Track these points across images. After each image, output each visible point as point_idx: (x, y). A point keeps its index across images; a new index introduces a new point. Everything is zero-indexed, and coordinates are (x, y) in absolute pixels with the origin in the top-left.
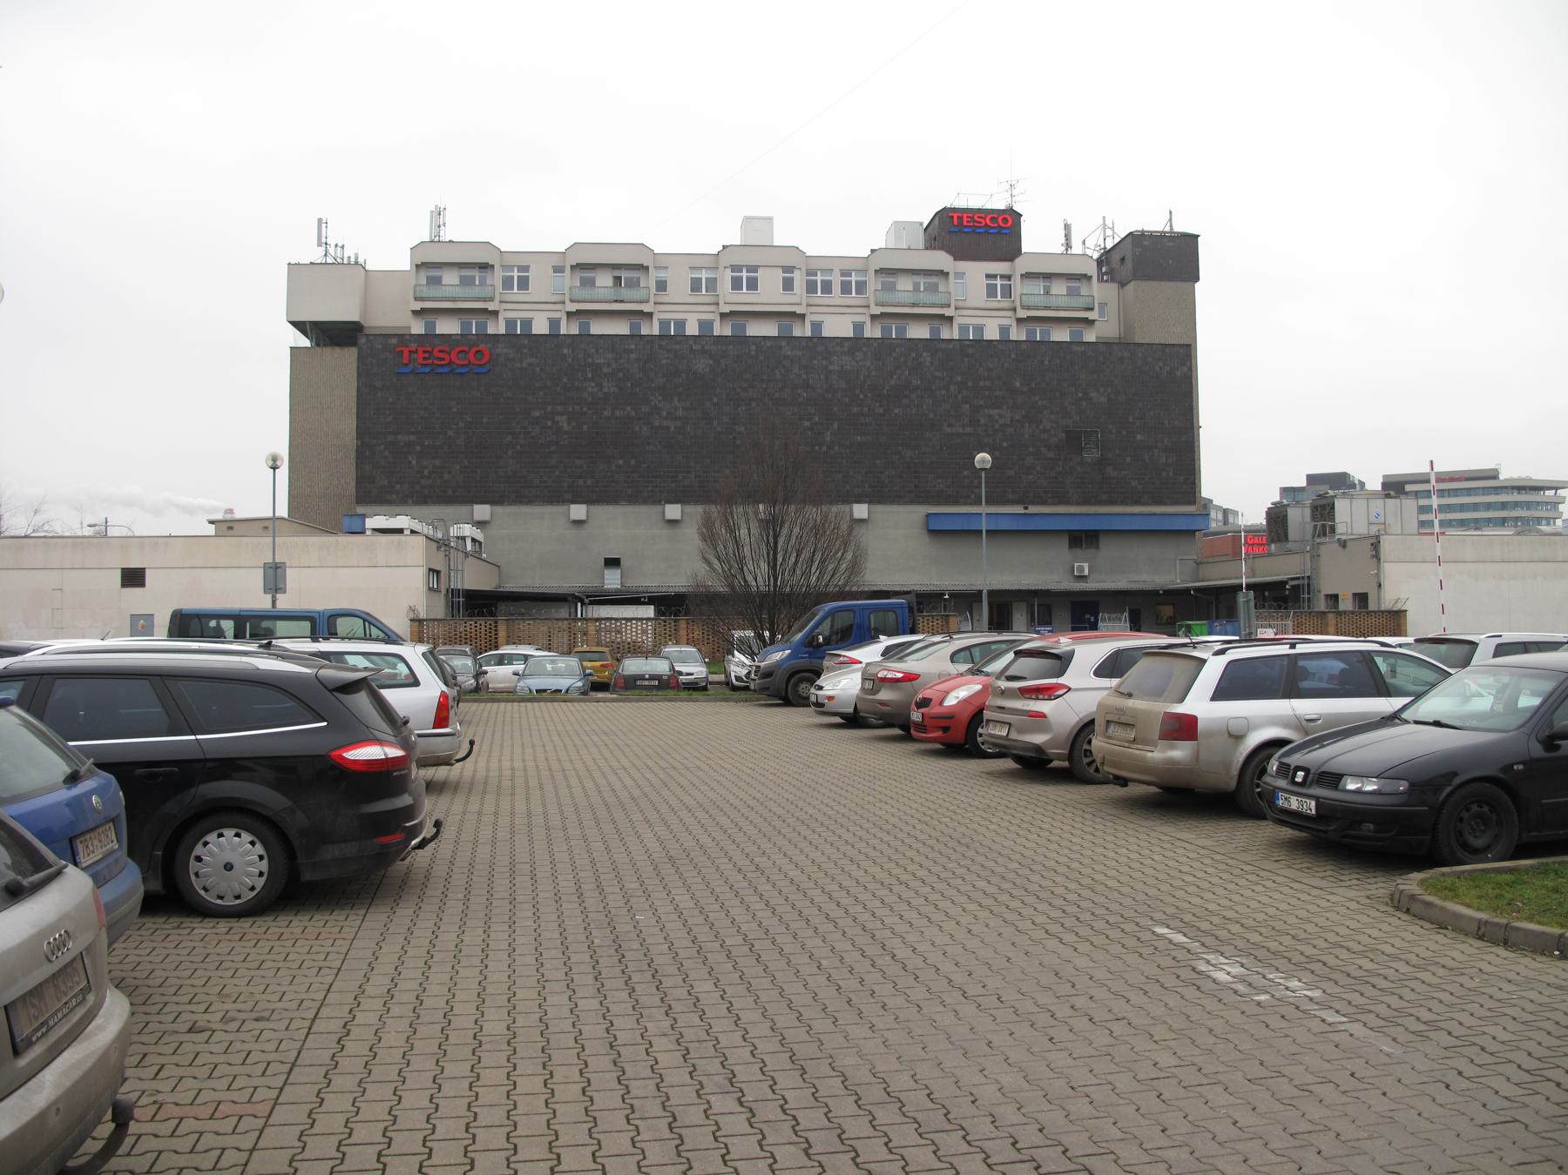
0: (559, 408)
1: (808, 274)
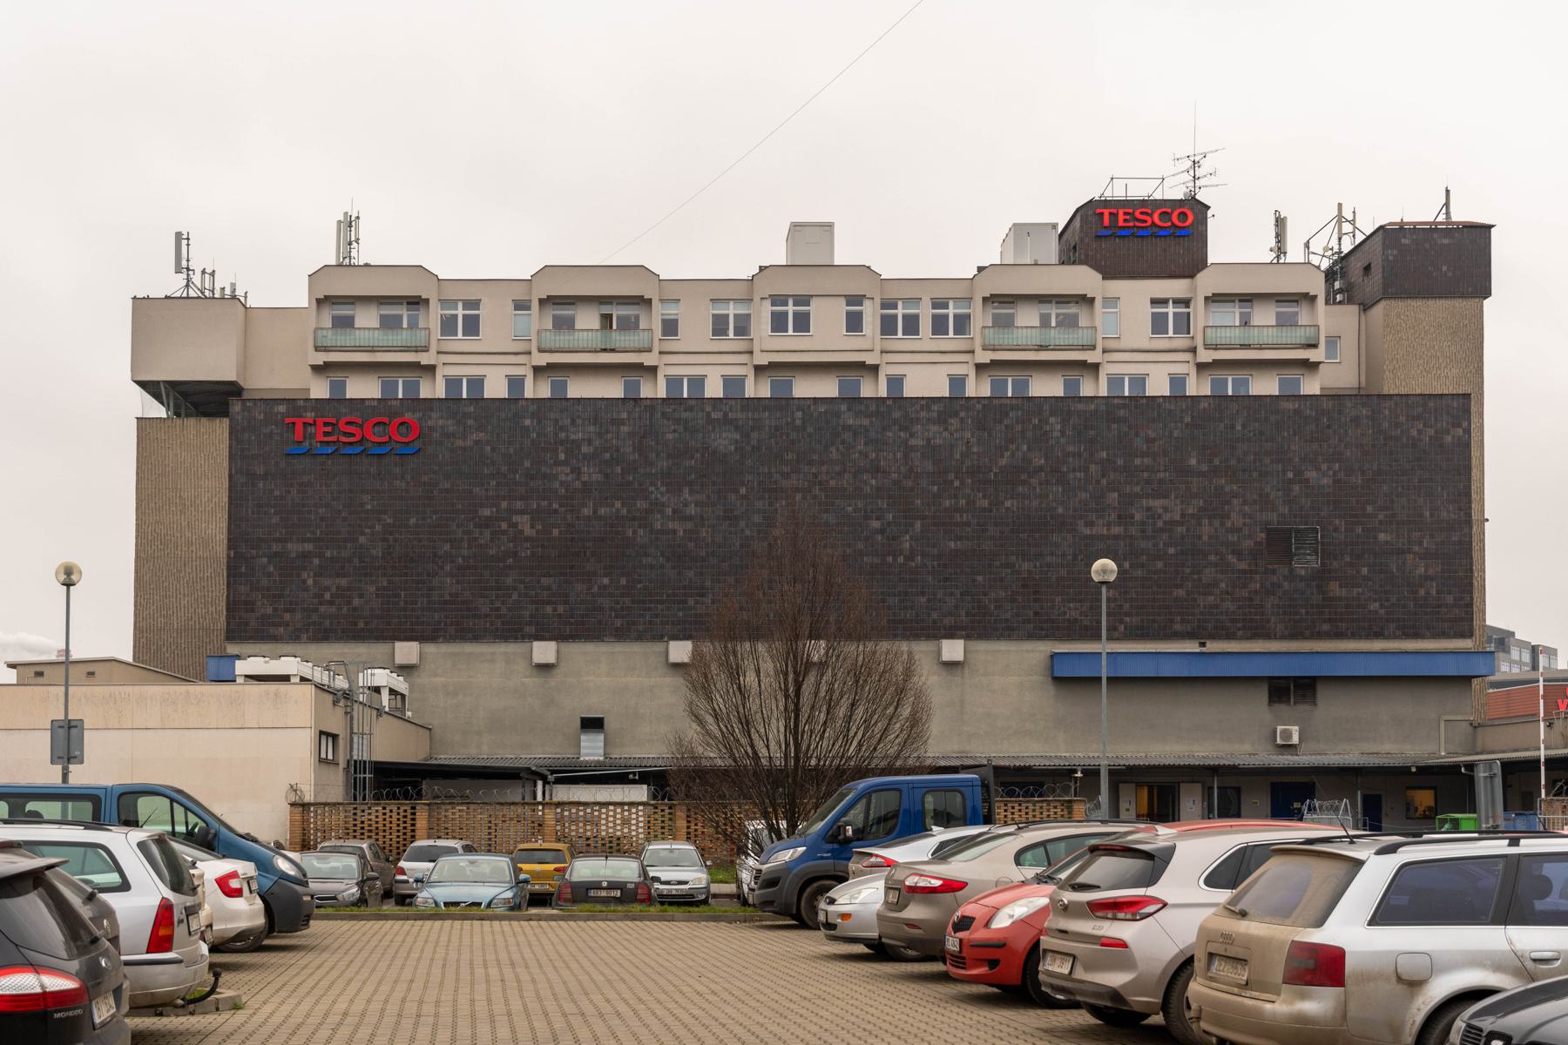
0: (519, 505)
1: (883, 306)
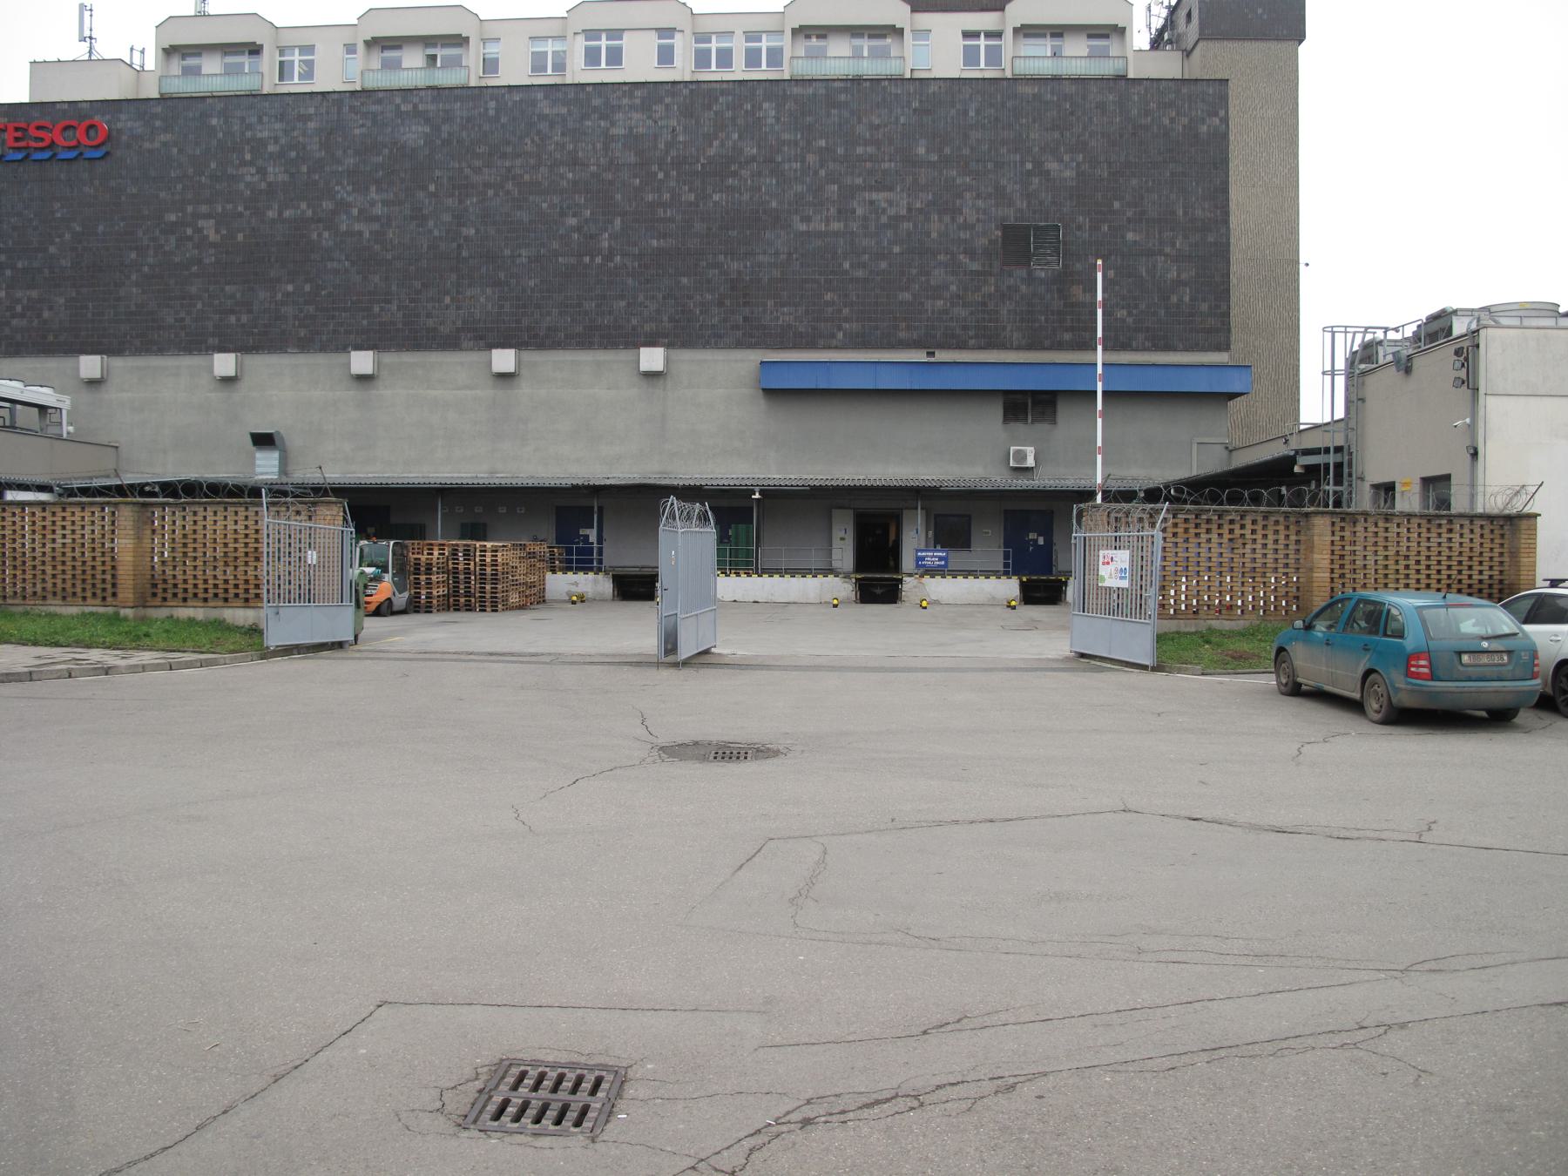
0: (204, 209)
